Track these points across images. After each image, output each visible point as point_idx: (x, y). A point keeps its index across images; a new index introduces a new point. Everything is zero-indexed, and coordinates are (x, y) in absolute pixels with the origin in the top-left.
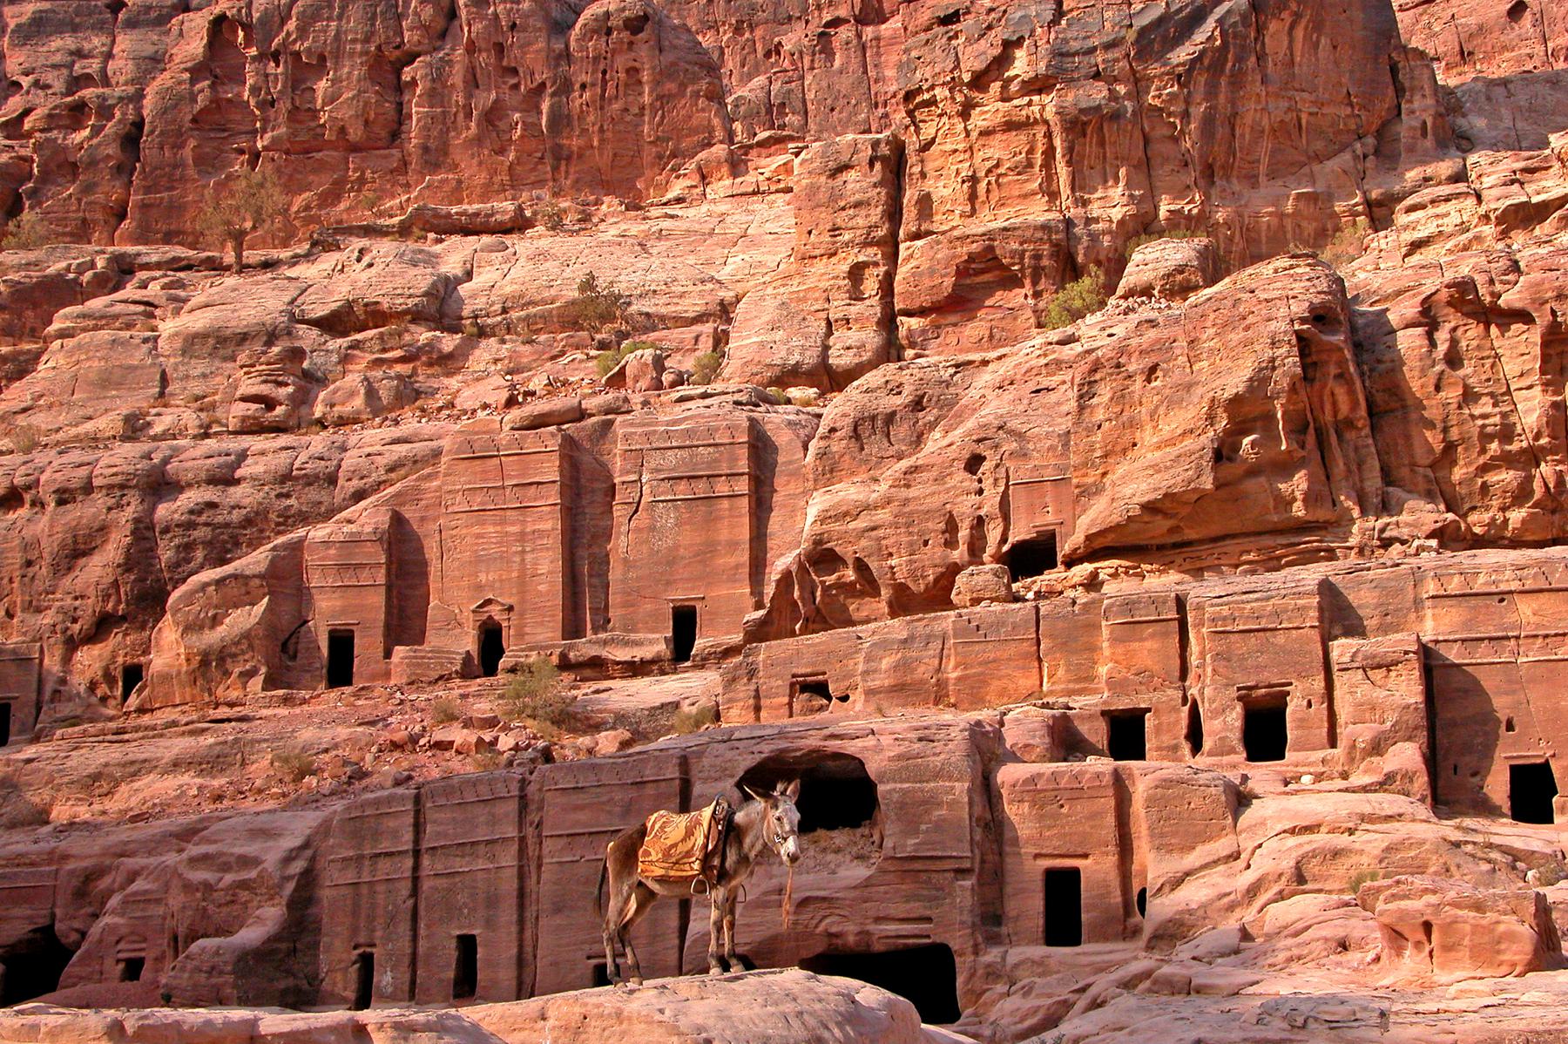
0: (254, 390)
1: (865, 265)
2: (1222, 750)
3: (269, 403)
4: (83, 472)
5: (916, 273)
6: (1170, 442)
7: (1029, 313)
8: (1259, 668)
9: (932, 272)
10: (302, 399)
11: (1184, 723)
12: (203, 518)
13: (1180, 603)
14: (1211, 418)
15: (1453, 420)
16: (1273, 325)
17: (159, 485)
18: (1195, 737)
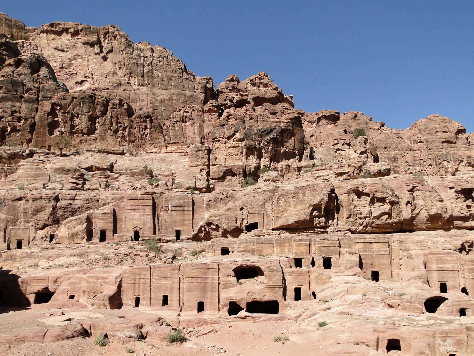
0: (73, 181)
1: (204, 169)
2: (319, 266)
3: (77, 184)
4: (39, 195)
5: (215, 172)
6: (300, 210)
7: (237, 181)
8: (327, 253)
9: (218, 172)
10: (84, 184)
11: (311, 261)
12: (69, 207)
13: (310, 240)
14: (309, 207)
15: (352, 211)
16: (323, 192)
17: (57, 199)
18: (313, 264)
